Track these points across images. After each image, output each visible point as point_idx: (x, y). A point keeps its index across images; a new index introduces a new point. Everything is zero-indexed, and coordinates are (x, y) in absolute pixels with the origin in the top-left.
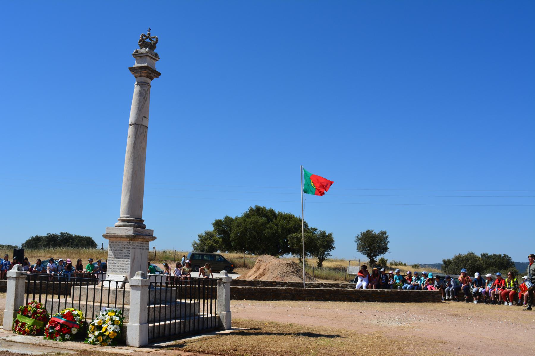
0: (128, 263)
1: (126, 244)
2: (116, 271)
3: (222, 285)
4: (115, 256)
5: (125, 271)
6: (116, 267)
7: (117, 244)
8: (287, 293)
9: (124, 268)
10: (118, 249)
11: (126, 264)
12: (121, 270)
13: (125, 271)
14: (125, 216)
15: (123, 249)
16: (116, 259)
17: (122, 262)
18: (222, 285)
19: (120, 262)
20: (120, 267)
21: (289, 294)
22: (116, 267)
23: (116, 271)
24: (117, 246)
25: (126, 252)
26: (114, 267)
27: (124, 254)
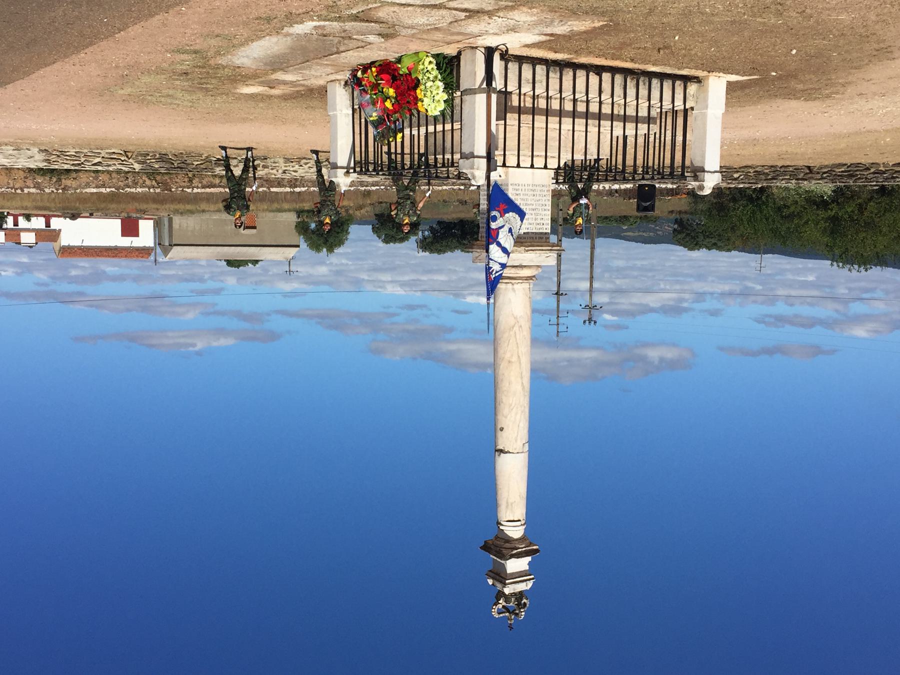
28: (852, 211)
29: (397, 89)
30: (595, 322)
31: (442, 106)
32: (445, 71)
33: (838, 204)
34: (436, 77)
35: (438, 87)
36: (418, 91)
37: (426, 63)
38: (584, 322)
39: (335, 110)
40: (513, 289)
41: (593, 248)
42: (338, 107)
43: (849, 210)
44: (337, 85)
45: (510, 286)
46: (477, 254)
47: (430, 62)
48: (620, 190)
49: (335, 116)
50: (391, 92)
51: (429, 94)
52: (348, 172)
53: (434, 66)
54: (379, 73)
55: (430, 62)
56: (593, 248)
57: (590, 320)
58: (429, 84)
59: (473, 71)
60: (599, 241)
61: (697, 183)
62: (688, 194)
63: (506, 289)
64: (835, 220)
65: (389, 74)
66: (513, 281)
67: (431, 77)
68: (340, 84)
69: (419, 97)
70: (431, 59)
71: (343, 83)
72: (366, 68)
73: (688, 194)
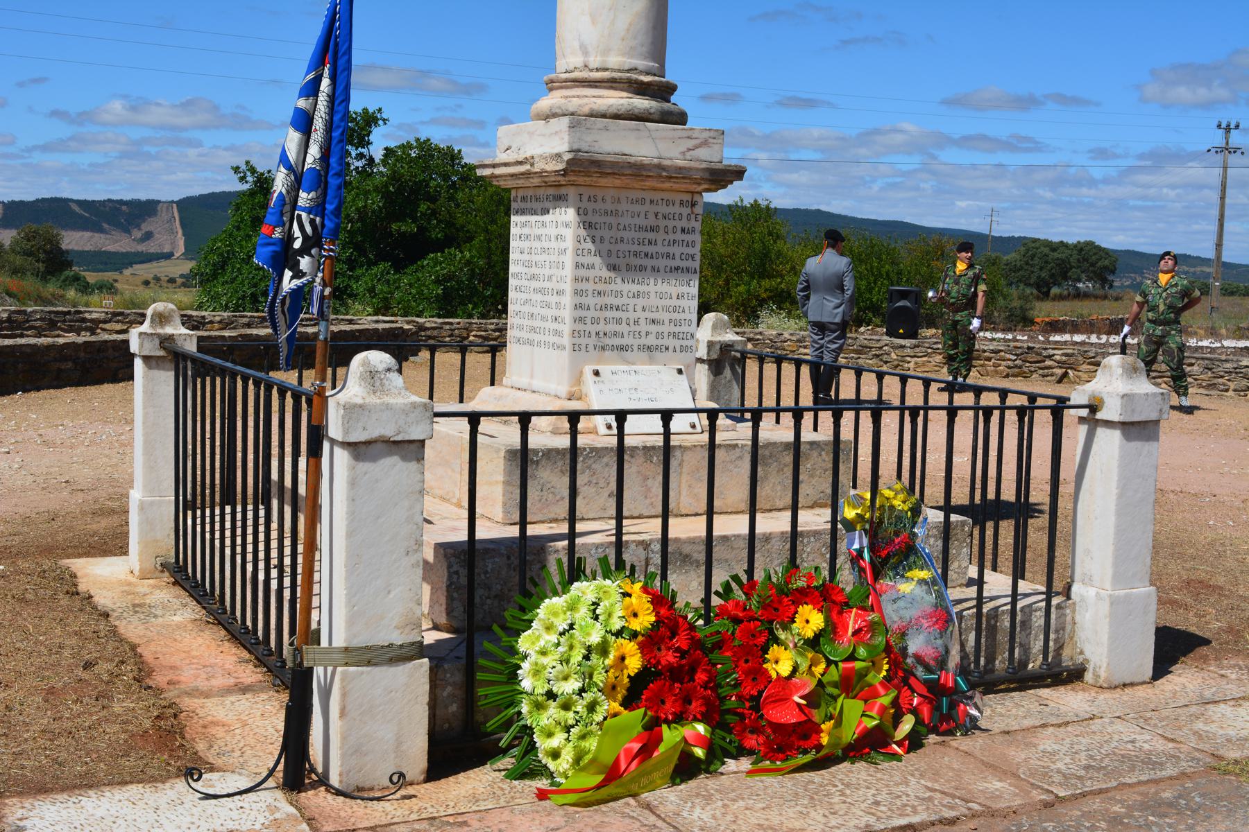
0: (683, 303)
1: (677, 209)
2: (621, 348)
3: (727, 372)
4: (613, 268)
5: (671, 342)
6: (623, 328)
7: (624, 206)
8: (65, 359)
9: (666, 329)
10: (627, 235)
11: (675, 309)
12: (651, 341)
13: (671, 342)
14: (642, 64)
15: (660, 236)
16: (619, 286)
17: (654, 301)
18: (727, 372)
19: (640, 302)
20: (643, 327)
21: (70, 365)
22: (623, 328)
23: (621, 348)
24: (626, 220)
25: (676, 250)
26: (611, 328)
27: (661, 263)
28: (738, 285)
29: (758, 673)
30: (1219, 126)
31: (551, 609)
32: (508, 724)
33: (757, 297)
34: (539, 706)
35: (536, 673)
36: (634, 663)
37: (567, 756)
38: (1237, 126)
39: (1114, 602)
40: (586, 53)
41: (1219, 246)
42: (1105, 608)
43: (742, 288)
44: (1103, 674)
45: (595, 62)
46: (703, 153)
47: (555, 755)
48: (1073, 332)
49: (1118, 579)
50: (781, 662)
51: (577, 656)
52: (1093, 408)
53: (544, 744)
54: (808, 730)
55: (555, 755)
56: (1219, 246)
57: (1228, 129)
58: (573, 685)
59: (378, 717)
60: (1210, 254)
61: (169, 330)
62: (1032, 322)
63: (606, 52)
64: (763, 272)
65: (778, 728)
66: (585, 74)
67: (553, 710)
68: (1097, 676)
69: (630, 647)
70: (552, 765)
71: (1088, 677)
72: (871, 745)
73: (1032, 322)
